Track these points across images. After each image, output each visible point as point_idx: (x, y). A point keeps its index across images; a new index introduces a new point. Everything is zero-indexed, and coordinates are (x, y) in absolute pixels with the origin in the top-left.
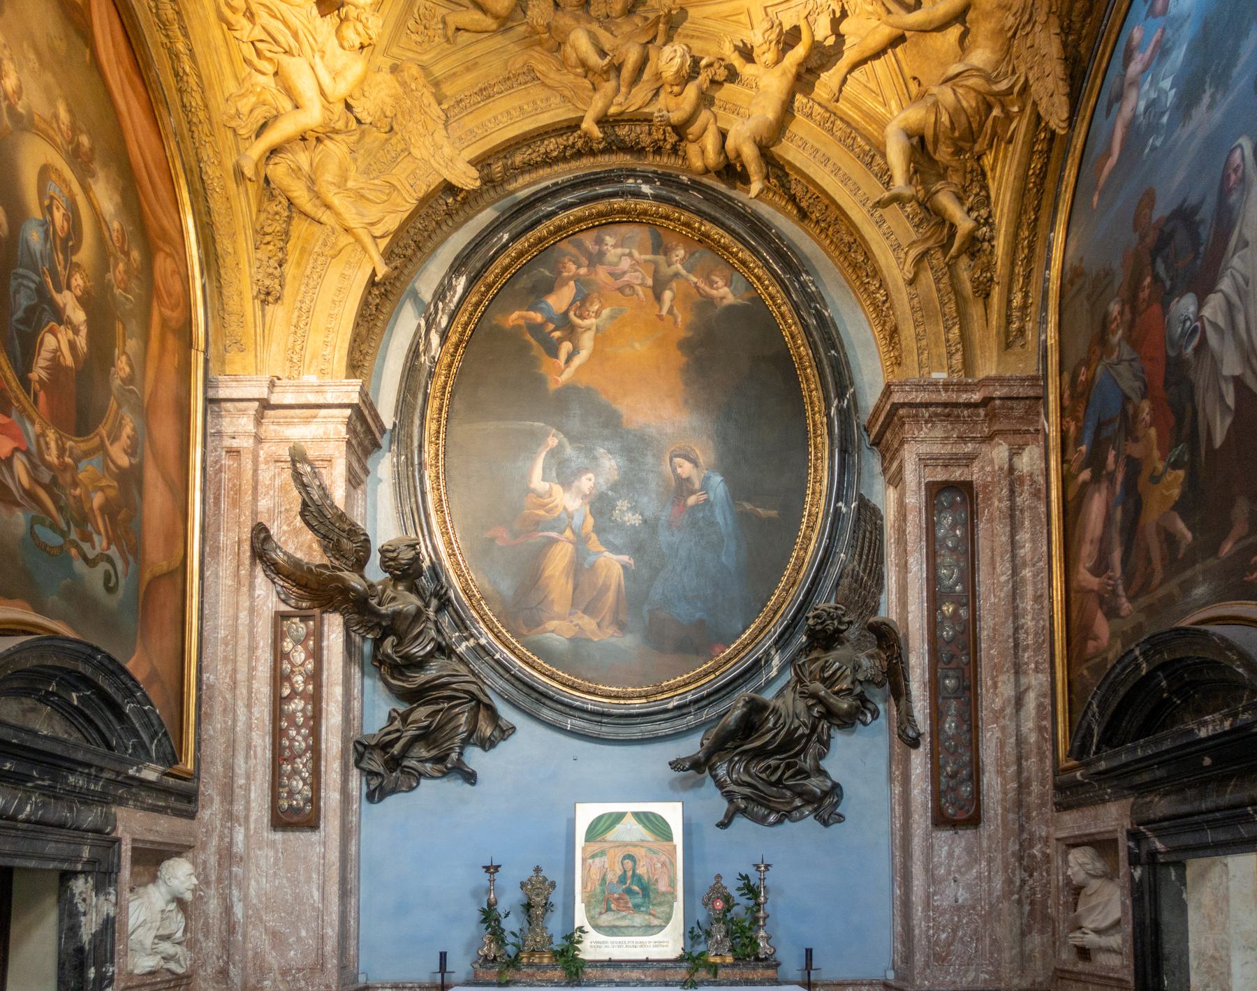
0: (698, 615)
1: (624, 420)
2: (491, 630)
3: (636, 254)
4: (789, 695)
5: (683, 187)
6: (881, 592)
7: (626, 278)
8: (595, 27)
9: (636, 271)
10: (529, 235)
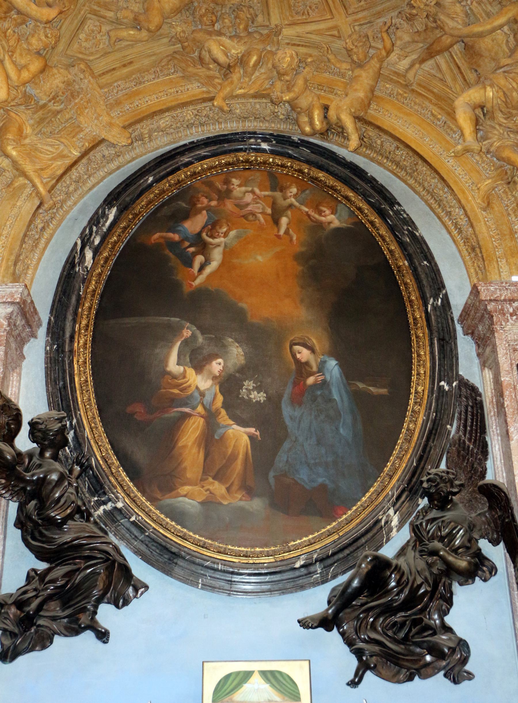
0: (320, 480)
1: (249, 316)
2: (128, 495)
3: (257, 191)
4: (411, 554)
5: (295, 145)
6: (486, 459)
7: (249, 208)
9: (257, 203)
10: (169, 178)
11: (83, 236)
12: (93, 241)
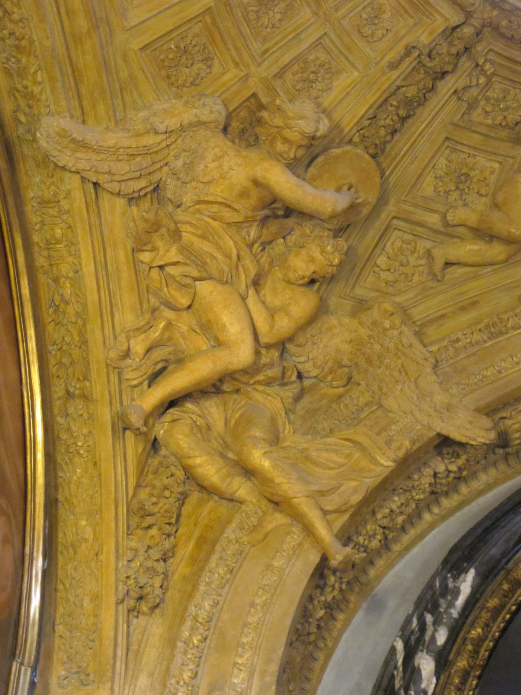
11: (407, 633)
12: (433, 638)
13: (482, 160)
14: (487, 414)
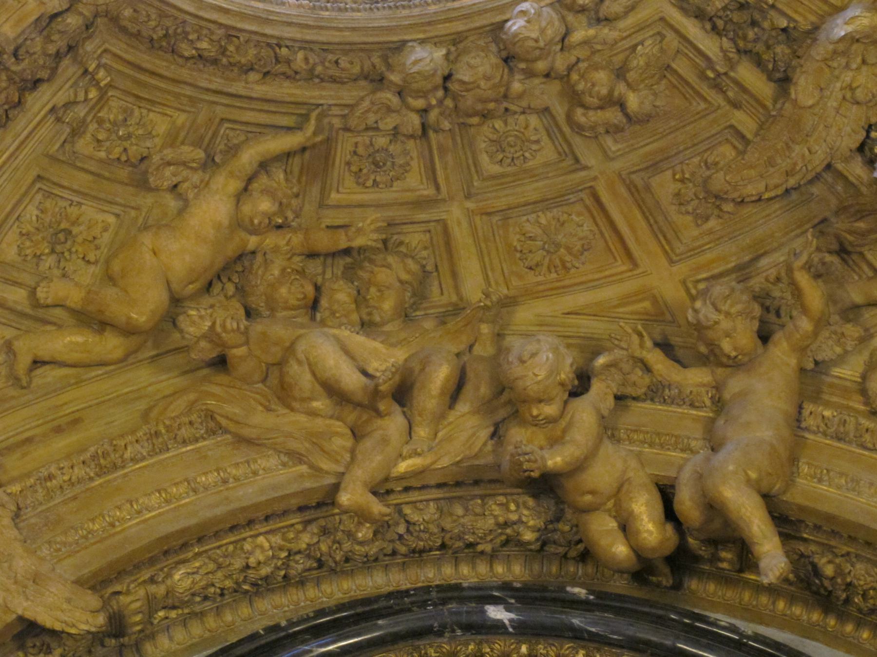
8: (344, 333)
13: (89, 211)
14: (93, 588)
